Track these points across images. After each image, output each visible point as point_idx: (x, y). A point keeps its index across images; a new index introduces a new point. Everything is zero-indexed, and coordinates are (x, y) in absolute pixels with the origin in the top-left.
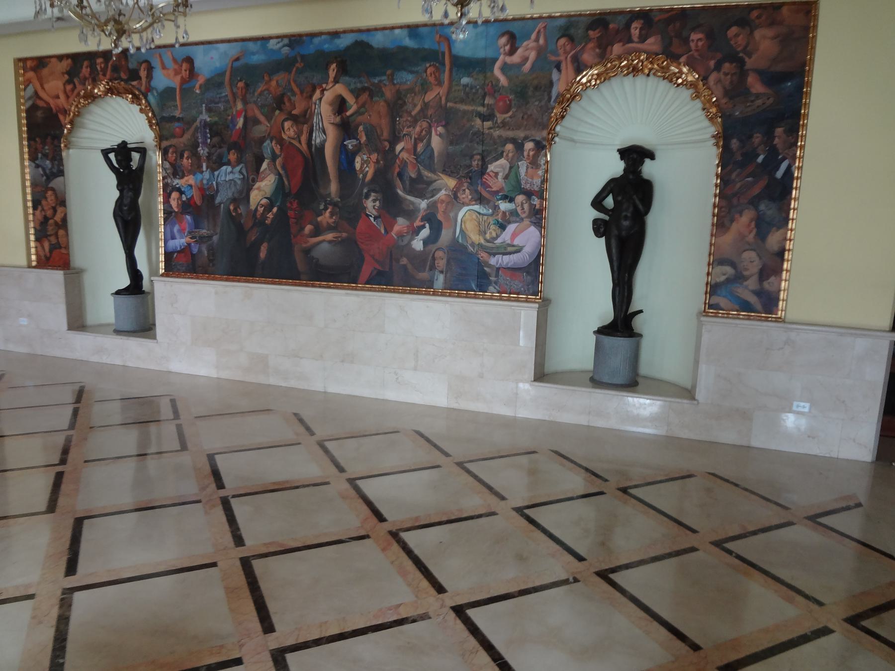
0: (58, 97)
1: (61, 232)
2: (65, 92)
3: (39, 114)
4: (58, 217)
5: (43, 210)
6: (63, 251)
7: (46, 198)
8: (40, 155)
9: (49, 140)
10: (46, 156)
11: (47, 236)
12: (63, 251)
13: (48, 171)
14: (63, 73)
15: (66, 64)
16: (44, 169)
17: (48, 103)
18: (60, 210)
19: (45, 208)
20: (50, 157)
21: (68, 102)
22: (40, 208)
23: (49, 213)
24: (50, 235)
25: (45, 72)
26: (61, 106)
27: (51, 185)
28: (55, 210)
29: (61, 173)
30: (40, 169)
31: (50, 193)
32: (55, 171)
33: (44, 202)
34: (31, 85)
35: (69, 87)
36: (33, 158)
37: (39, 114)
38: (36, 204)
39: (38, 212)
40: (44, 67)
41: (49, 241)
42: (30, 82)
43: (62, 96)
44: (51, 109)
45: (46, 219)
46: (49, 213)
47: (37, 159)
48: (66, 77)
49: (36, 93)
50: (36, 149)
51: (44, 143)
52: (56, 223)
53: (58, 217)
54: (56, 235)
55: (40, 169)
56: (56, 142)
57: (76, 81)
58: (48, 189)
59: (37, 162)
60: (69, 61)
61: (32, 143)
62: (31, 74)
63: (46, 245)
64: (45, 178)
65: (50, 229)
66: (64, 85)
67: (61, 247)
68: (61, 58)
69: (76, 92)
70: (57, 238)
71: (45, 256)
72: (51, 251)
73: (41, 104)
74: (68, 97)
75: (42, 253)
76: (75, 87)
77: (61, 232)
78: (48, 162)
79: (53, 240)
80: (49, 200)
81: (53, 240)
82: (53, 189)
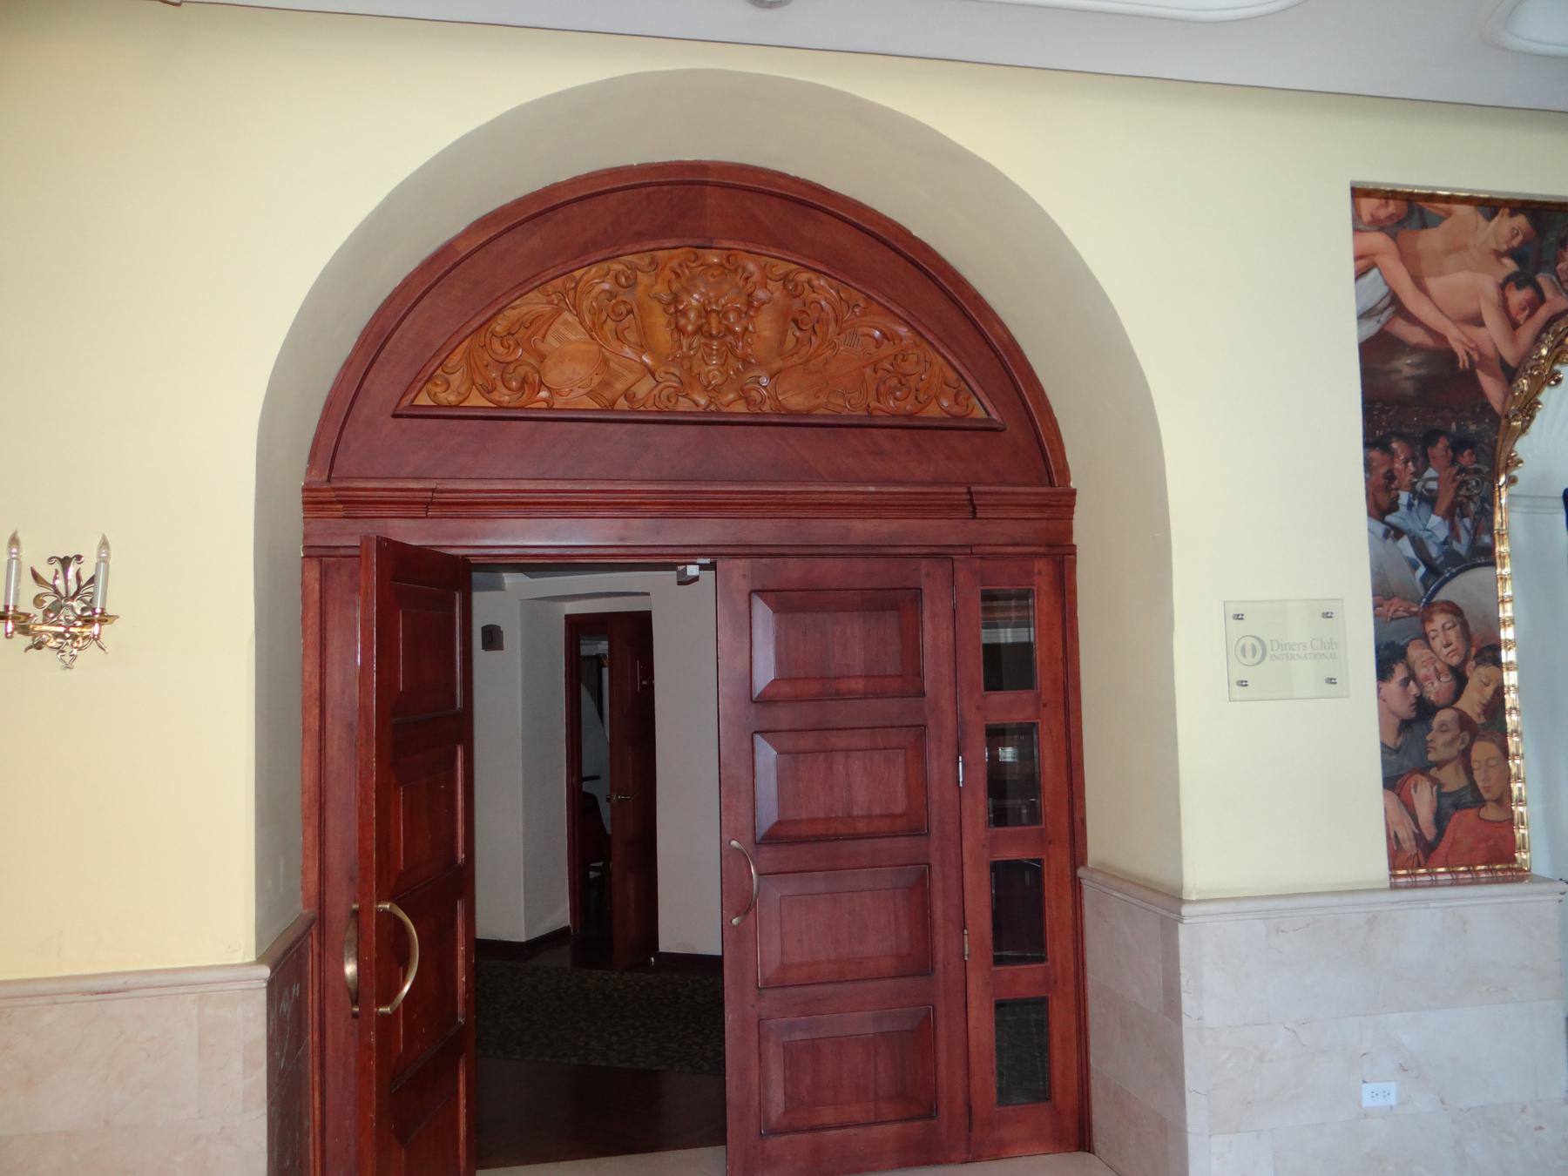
0: (1478, 321)
1: (1482, 751)
2: (1504, 306)
3: (1406, 366)
4: (1471, 702)
5: (1412, 676)
6: (1491, 813)
7: (1425, 638)
8: (1404, 497)
9: (1440, 448)
10: (1429, 500)
11: (1424, 769)
12: (1491, 813)
13: (1434, 551)
14: (1499, 255)
15: (1509, 228)
16: (1418, 544)
17: (1440, 337)
18: (1477, 675)
19: (1422, 673)
20: (1443, 504)
21: (1514, 340)
22: (1400, 672)
23: (1437, 689)
24: (1440, 765)
25: (1430, 240)
26: (1488, 350)
27: (1442, 596)
28: (1460, 679)
29: (1484, 556)
30: (1405, 543)
31: (1440, 620)
32: (1461, 547)
33: (1416, 653)
34: (1375, 272)
35: (1518, 297)
36: (1380, 505)
37: (1406, 366)
38: (1388, 658)
39: (1394, 685)
40: (1424, 225)
41: (1434, 781)
42: (1373, 265)
43: (1492, 319)
44: (1452, 356)
45: (1425, 708)
46: (1437, 689)
47: (1393, 507)
48: (1510, 266)
49: (1394, 300)
50: (1390, 476)
51: (1422, 461)
52: (1464, 722)
53: (1471, 702)
54: (1465, 755)
55: (1405, 543)
56: (1466, 457)
57: (1543, 279)
58: (1429, 608)
59: (1389, 518)
60: (1521, 221)
61: (1375, 454)
62: (1377, 240)
63: (1424, 798)
64: (1422, 570)
65: (1441, 738)
66: (1502, 287)
67: (1479, 802)
68: (1490, 206)
69: (1543, 314)
70: (1469, 771)
71: (1419, 837)
72: (1440, 819)
73: (1414, 335)
74: (1515, 325)
75: (1406, 833)
76: (1540, 299)
77: (1482, 751)
78: (1435, 520)
79: (1452, 779)
80: (1437, 644)
81: (1452, 779)
82: (1453, 609)
